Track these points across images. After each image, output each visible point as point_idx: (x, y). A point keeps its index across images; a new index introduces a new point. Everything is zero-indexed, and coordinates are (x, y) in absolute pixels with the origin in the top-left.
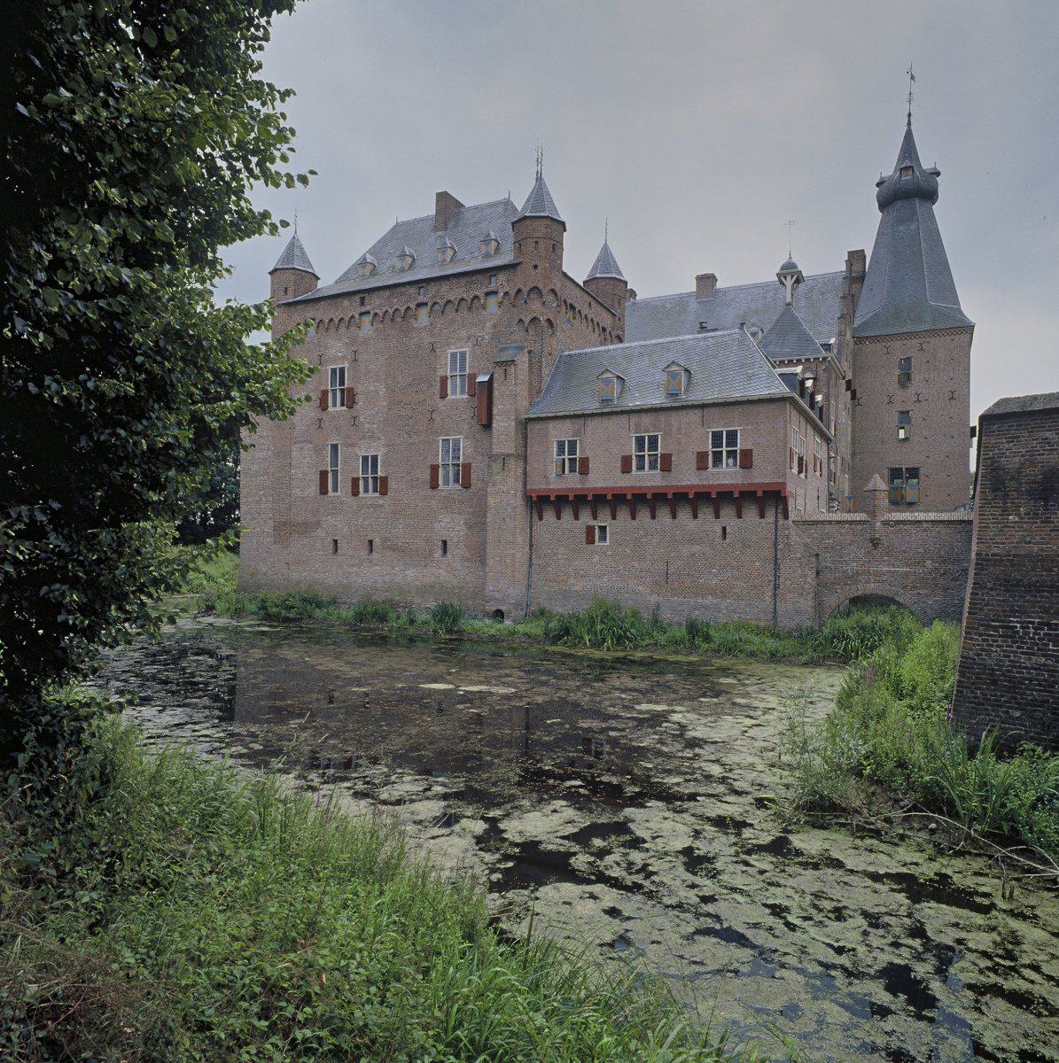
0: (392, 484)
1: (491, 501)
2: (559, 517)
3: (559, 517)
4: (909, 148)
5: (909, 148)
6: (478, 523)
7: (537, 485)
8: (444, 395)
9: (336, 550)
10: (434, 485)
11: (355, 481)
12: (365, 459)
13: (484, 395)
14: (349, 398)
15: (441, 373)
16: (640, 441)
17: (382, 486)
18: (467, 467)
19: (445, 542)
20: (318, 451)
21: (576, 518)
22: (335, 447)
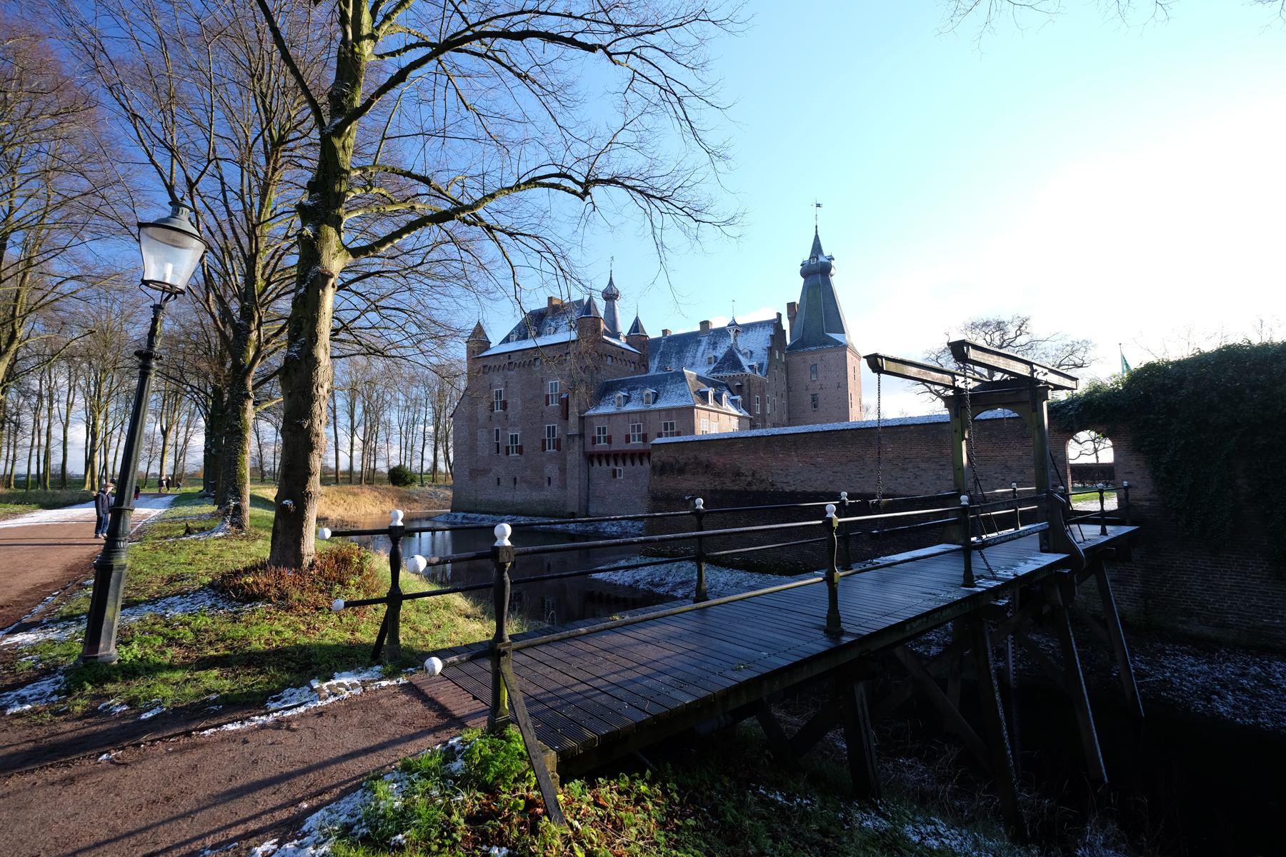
0: (525, 449)
1: (568, 458)
2: (600, 465)
3: (600, 465)
4: (817, 248)
5: (817, 248)
6: (563, 471)
7: (589, 448)
8: (547, 404)
9: (499, 483)
10: (544, 449)
11: (508, 448)
12: (512, 436)
13: (565, 404)
14: (504, 405)
15: (546, 393)
16: (633, 427)
17: (520, 450)
18: (559, 440)
19: (549, 478)
20: (490, 432)
21: (608, 465)
22: (497, 431)
